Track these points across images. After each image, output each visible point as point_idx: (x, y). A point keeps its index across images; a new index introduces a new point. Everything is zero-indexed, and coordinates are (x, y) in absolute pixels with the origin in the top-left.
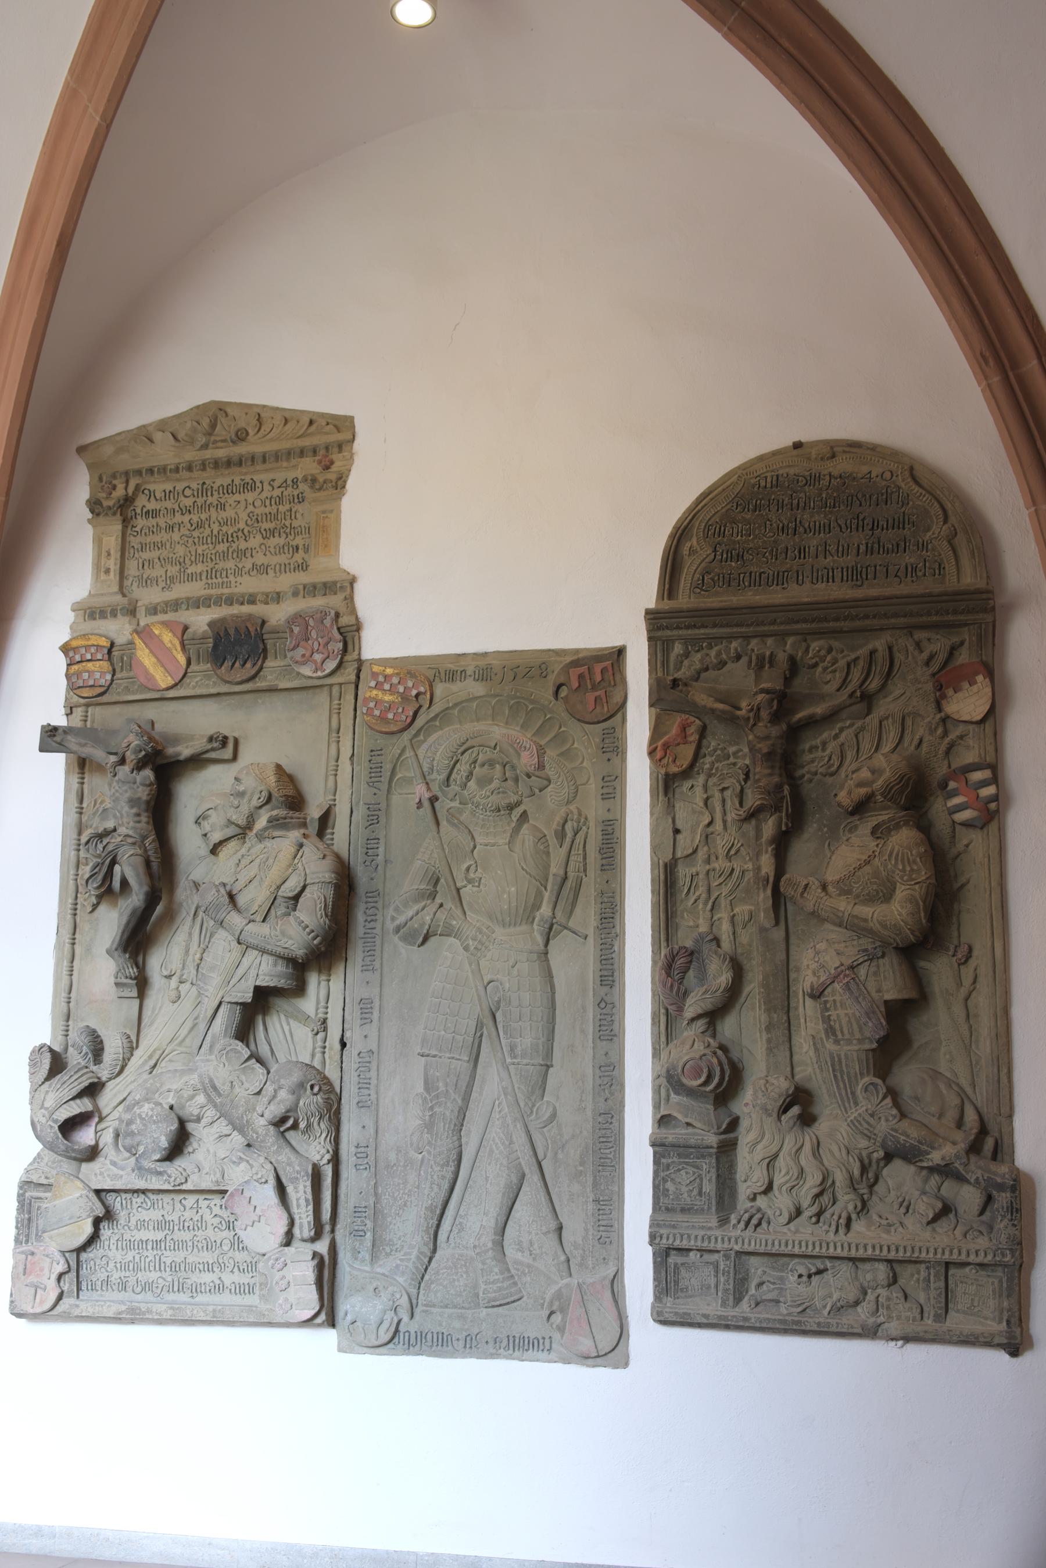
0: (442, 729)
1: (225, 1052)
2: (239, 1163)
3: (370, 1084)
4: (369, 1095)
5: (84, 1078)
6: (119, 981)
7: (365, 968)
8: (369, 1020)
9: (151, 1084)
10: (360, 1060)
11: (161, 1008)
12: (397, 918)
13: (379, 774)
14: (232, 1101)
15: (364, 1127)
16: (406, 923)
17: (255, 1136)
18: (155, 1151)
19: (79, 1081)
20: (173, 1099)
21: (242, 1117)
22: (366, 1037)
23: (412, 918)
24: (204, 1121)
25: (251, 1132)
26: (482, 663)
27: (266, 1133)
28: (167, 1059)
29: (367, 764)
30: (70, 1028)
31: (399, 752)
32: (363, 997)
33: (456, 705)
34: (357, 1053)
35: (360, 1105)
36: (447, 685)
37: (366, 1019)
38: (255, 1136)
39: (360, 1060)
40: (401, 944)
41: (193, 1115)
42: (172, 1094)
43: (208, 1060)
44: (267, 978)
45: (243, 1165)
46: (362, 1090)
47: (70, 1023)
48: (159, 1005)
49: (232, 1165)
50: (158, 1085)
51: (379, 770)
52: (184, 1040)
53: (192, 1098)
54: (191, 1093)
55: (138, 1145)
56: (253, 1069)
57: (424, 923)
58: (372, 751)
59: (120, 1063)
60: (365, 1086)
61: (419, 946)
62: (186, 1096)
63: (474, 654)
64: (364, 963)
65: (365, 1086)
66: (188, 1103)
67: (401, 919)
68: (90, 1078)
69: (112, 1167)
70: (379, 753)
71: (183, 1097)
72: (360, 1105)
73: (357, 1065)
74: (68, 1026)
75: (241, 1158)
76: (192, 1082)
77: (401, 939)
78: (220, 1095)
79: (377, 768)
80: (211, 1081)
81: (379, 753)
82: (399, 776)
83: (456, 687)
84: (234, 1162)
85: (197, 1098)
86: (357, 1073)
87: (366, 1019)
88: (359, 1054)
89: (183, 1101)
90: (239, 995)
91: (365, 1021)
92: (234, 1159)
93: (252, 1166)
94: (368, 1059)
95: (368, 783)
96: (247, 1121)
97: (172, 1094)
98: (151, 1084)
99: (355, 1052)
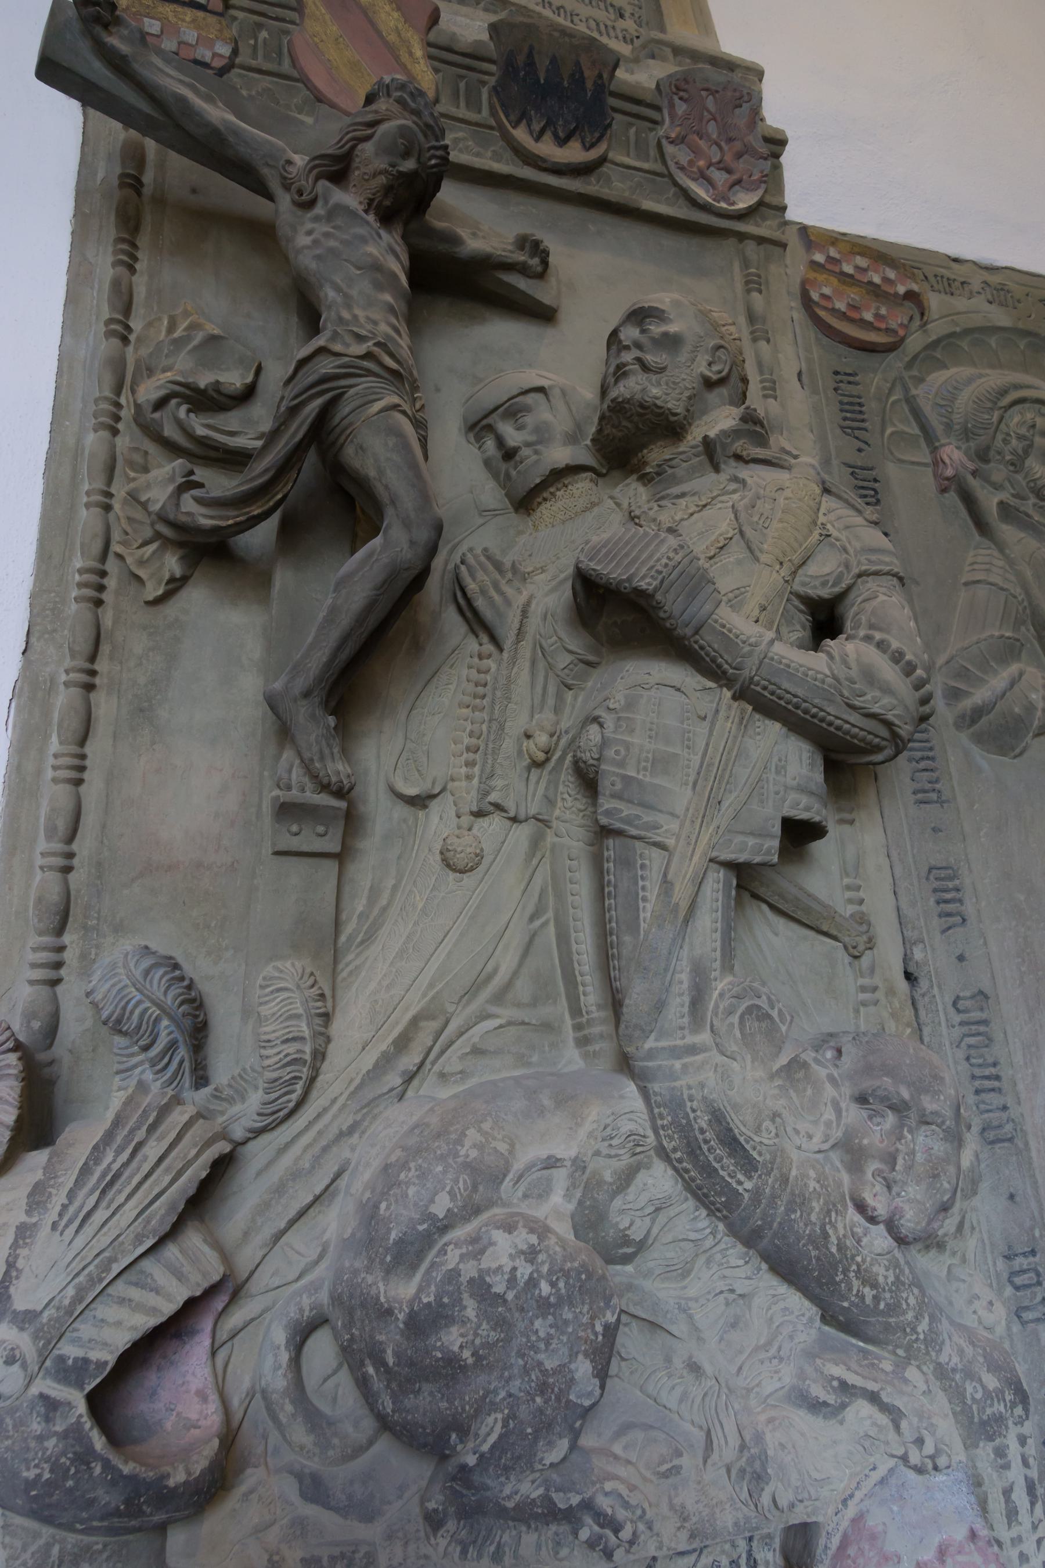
0: (945, 367)
1: (735, 1019)
2: (843, 1406)
3: (998, 1078)
4: (1005, 1108)
5: (187, 1147)
6: (294, 795)
7: (920, 796)
8: (958, 919)
9: (480, 1147)
10: (964, 1017)
11: (395, 888)
12: (967, 694)
13: (861, 417)
14: (785, 1180)
15: (1012, 1197)
16: (995, 704)
17: (868, 1293)
18: (549, 1426)
19: (175, 1160)
20: (568, 1196)
21: (826, 1236)
22: (961, 958)
23: (1004, 694)
24: (654, 1258)
25: (856, 1284)
26: (995, 279)
27: (897, 1278)
28: (462, 1046)
29: (831, 393)
30: (67, 955)
31: (888, 385)
32: (933, 863)
33: (967, 332)
34: (949, 999)
35: (991, 1135)
36: (947, 298)
37: (949, 915)
38: (868, 1293)
39: (964, 1017)
40: (976, 751)
41: (626, 1241)
42: (560, 1177)
43: (693, 1050)
44: (805, 800)
45: (862, 1410)
46: (983, 1095)
47: (67, 938)
48: (390, 882)
49: (810, 1418)
50: (503, 1147)
51: (857, 408)
52: (509, 985)
53: (627, 1177)
54: (626, 1160)
55: (478, 1412)
56: (805, 1065)
57: (1030, 708)
58: (836, 373)
59: (305, 1072)
60: (988, 1084)
61: (1015, 757)
62: (608, 1176)
63: (974, 263)
64: (919, 786)
65: (988, 1084)
66: (617, 1203)
67: (980, 696)
68: (208, 1144)
69: (311, 1511)
70: (851, 379)
71: (600, 1183)
72: (991, 1135)
73: (957, 1032)
74: (61, 949)
75: (844, 1385)
76: (626, 1127)
77: (979, 739)
78: (749, 1165)
79: (851, 404)
80: (717, 1117)
81: (851, 379)
82: (889, 431)
83: (960, 303)
84: (816, 1406)
85: (641, 1177)
86: (961, 1054)
87: (949, 915)
88: (955, 1004)
89: (601, 1196)
90: (751, 841)
91: (951, 920)
92: (818, 1391)
93: (894, 1414)
94: (976, 1015)
95: (842, 428)
96: (841, 1247)
97: (560, 1177)
98: (480, 1147)
99: (943, 1000)
